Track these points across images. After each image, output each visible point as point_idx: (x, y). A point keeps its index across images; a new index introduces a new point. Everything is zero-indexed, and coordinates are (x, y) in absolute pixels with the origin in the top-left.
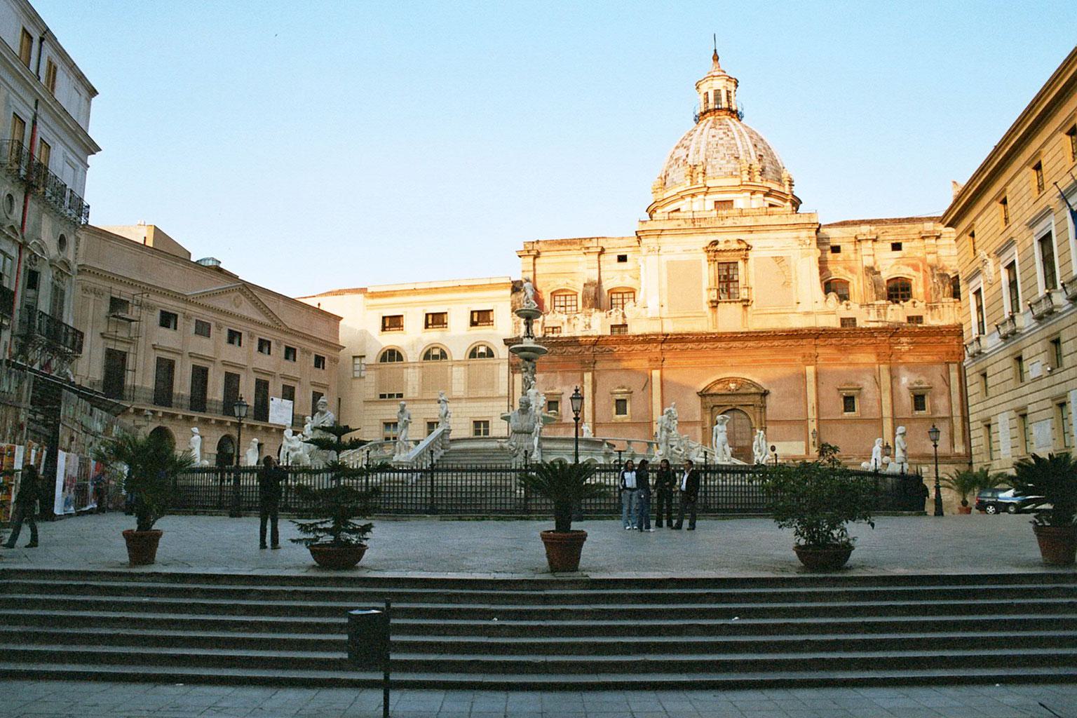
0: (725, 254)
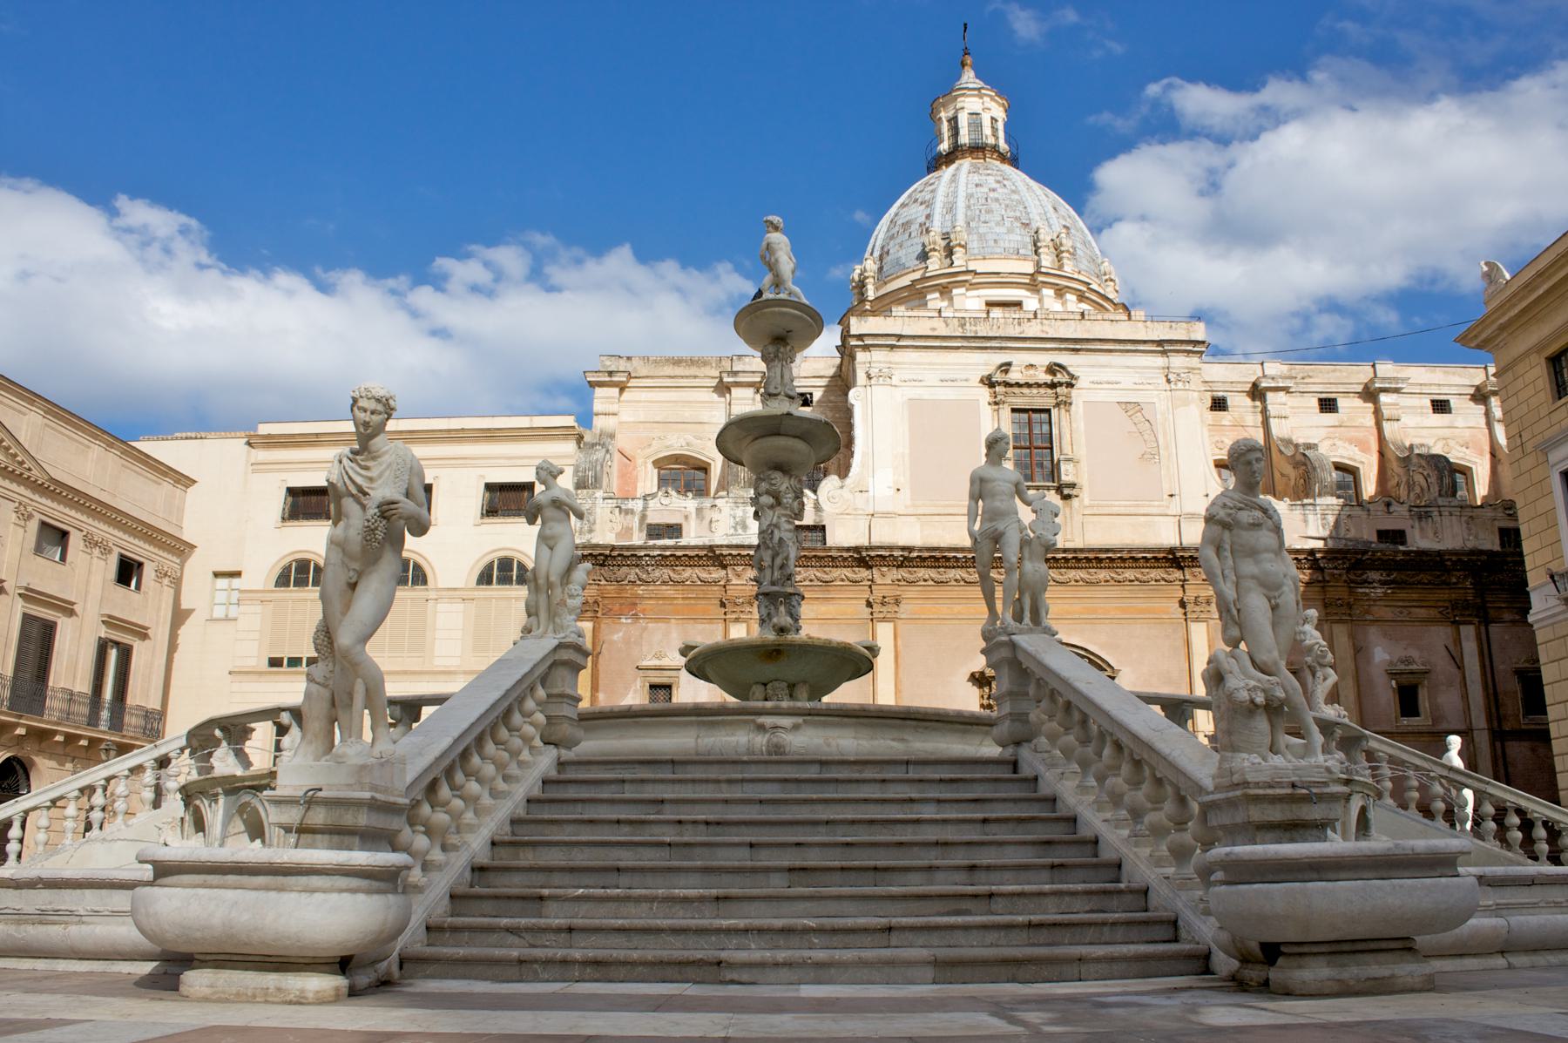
0: (1026, 391)
